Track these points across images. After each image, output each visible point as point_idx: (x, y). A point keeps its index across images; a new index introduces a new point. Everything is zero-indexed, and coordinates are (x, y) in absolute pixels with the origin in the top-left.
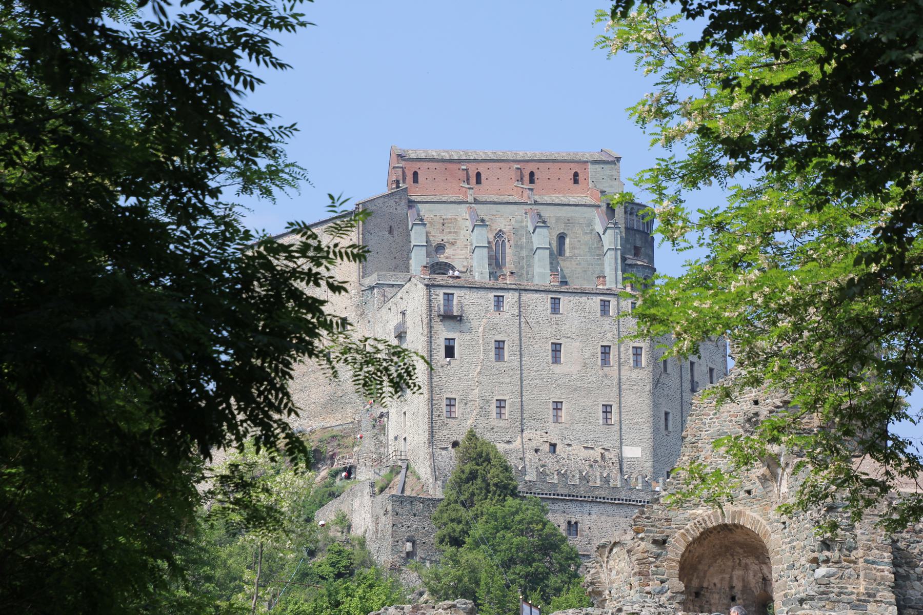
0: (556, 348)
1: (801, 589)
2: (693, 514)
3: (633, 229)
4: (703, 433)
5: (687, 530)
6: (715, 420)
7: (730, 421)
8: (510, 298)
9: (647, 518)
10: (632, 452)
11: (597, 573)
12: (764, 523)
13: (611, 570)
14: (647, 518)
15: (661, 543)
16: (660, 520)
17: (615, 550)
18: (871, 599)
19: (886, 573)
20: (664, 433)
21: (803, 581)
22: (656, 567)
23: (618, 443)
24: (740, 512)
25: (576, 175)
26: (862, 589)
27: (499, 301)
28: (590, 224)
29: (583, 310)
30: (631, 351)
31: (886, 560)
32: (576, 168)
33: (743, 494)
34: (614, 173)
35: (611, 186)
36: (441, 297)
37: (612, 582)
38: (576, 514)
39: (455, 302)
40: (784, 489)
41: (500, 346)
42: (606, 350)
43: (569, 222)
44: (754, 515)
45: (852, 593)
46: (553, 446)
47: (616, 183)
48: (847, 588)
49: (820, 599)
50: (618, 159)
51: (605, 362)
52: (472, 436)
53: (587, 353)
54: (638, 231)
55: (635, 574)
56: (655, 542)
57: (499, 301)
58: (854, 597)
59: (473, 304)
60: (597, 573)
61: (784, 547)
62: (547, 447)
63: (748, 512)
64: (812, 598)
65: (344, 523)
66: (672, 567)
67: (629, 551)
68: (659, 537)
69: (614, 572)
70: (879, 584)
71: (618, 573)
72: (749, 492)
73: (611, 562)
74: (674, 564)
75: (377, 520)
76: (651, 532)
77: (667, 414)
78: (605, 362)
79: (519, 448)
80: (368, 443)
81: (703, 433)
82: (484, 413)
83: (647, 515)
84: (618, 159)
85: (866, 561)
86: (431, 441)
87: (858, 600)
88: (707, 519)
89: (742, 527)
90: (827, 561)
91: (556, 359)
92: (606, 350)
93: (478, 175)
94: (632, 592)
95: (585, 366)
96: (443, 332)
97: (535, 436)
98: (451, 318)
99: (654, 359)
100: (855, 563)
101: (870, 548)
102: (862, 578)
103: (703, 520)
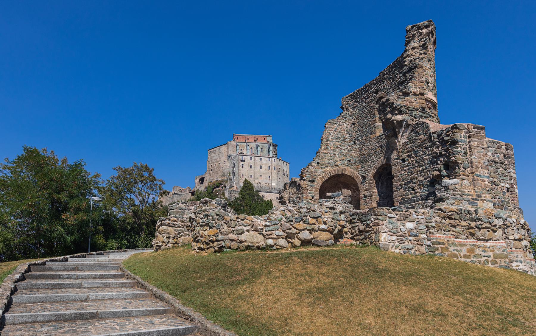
18: (479, 199)
31: (486, 175)
45: (469, 195)
48: (465, 192)
49: (452, 199)
58: (470, 197)
70: (483, 189)
87: (473, 199)
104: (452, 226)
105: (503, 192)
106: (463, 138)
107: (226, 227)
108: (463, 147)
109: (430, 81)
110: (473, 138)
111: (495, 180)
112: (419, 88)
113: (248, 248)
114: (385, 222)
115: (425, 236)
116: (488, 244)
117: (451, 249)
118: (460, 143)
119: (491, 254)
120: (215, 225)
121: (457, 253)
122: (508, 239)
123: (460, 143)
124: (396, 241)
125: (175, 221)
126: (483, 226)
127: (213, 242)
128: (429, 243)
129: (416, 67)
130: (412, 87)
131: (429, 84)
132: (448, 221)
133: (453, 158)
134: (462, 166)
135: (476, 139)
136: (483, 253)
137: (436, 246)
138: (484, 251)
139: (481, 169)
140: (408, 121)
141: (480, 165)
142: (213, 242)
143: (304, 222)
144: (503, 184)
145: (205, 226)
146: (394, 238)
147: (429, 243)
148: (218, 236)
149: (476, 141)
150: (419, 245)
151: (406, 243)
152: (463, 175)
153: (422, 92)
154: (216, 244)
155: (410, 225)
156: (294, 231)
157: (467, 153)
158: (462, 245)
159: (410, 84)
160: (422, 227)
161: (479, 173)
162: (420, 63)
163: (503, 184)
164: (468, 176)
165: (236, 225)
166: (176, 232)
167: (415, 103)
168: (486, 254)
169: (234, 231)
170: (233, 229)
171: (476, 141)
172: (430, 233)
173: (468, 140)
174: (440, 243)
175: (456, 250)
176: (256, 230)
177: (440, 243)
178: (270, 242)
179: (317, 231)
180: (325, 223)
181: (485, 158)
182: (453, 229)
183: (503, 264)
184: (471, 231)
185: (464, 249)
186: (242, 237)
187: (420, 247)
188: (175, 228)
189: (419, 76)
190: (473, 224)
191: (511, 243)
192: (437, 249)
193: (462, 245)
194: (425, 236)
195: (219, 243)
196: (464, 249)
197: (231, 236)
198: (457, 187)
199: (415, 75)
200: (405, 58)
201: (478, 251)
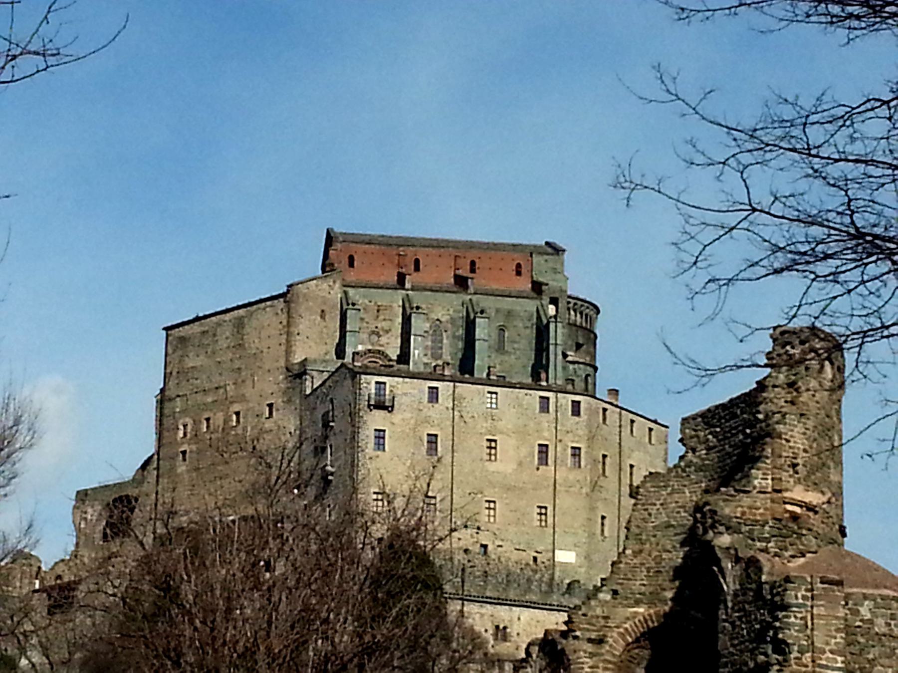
2: (636, 613)
3: (575, 325)
5: (626, 629)
6: (661, 510)
7: (678, 512)
9: (584, 615)
14: (584, 615)
15: (600, 641)
16: (598, 617)
20: (600, 538)
22: (590, 667)
23: (550, 547)
25: (519, 266)
29: (520, 405)
30: (569, 451)
31: (839, 665)
32: (519, 258)
34: (558, 266)
35: (553, 280)
36: (373, 386)
39: (387, 392)
41: (433, 439)
42: (543, 449)
43: (509, 314)
46: (485, 547)
47: (559, 276)
50: (564, 251)
53: (524, 451)
54: (581, 327)
56: (590, 640)
59: (406, 394)
62: (477, 548)
68: (593, 636)
74: (610, 666)
76: (588, 630)
77: (603, 518)
83: (584, 610)
84: (564, 251)
88: (648, 618)
92: (543, 449)
93: (417, 262)
95: (520, 464)
103: (644, 618)
106: (801, 601)
108: (799, 615)
109: (799, 461)
110: (818, 600)
112: (773, 479)
118: (794, 609)
123: (794, 609)
129: (769, 435)
130: (760, 479)
131: (799, 468)
133: (780, 636)
134: (796, 648)
135: (822, 603)
139: (831, 656)
140: (739, 551)
141: (827, 648)
149: (822, 605)
152: (796, 664)
153: (778, 488)
157: (807, 627)
159: (753, 471)
161: (824, 662)
162: (777, 426)
164: (807, 666)
167: (761, 511)
171: (822, 605)
173: (809, 603)
181: (838, 635)
189: (773, 453)
199: (765, 453)
200: (761, 403)
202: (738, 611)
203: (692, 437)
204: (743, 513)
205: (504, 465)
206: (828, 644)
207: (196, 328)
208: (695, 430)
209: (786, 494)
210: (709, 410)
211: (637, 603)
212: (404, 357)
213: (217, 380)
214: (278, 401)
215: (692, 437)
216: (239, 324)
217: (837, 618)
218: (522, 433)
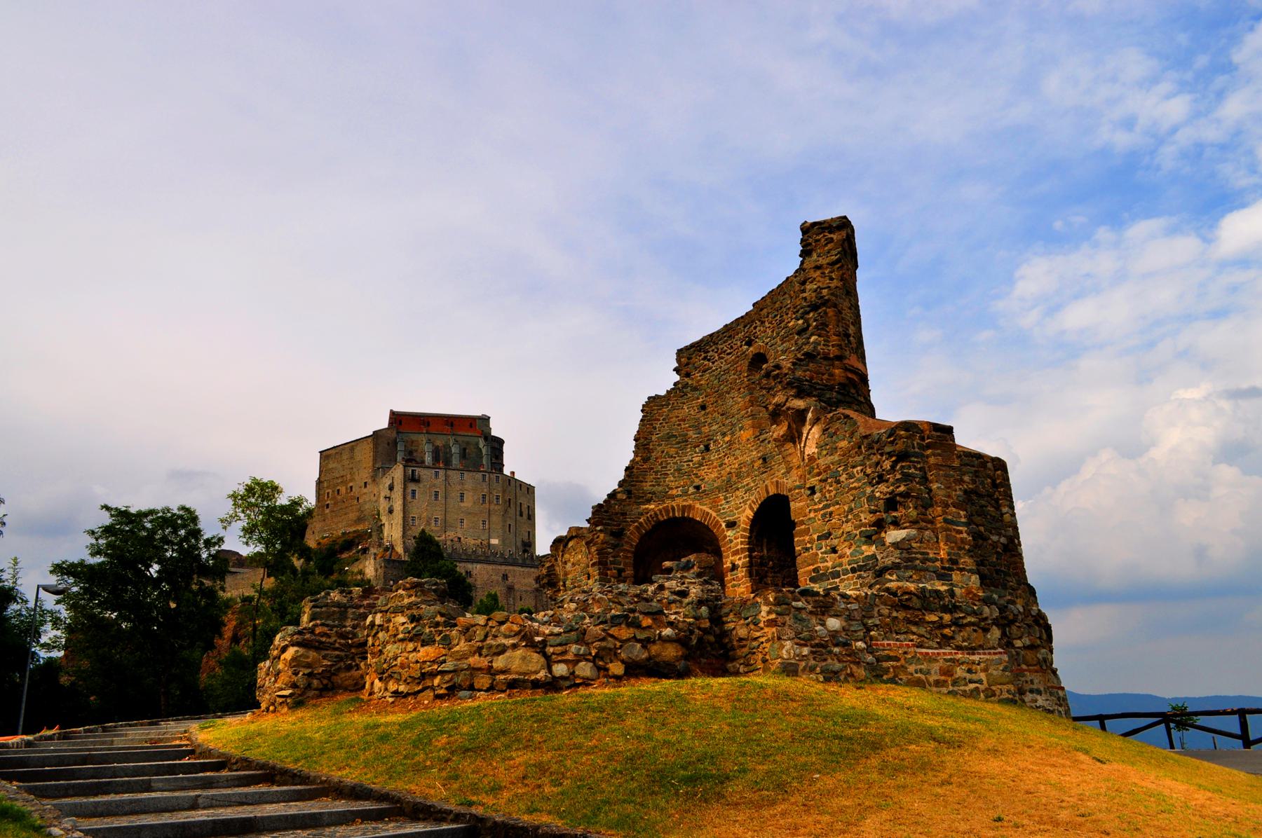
0: (462, 495)
1: (845, 560)
4: (654, 438)
8: (442, 473)
10: (494, 541)
11: (553, 566)
12: (714, 514)
13: (566, 563)
17: (571, 544)
19: (965, 535)
21: (849, 552)
24: (690, 506)
26: (943, 554)
27: (437, 474)
28: (477, 444)
33: (691, 490)
37: (566, 574)
38: (470, 566)
40: (811, 449)
43: (468, 443)
44: (704, 508)
49: (907, 568)
51: (484, 501)
52: (423, 531)
55: (593, 565)
56: (613, 534)
57: (437, 474)
58: (938, 564)
60: (553, 566)
61: (812, 515)
63: (698, 506)
64: (896, 567)
65: (361, 572)
66: (627, 557)
67: (587, 543)
69: (569, 565)
70: (960, 549)
71: (573, 564)
72: (697, 488)
73: (567, 556)
75: (376, 570)
78: (484, 501)
79: (444, 538)
80: (375, 538)
81: (654, 438)
82: (428, 523)
85: (946, 521)
86: (404, 536)
87: (943, 568)
89: (693, 520)
90: (896, 524)
91: (462, 500)
92: (484, 497)
94: (590, 582)
96: (412, 486)
97: (451, 534)
98: (414, 479)
99: (505, 501)
100: (932, 522)
101: (947, 506)
102: (942, 544)
104: (909, 622)
105: (997, 553)
107: (462, 643)
111: (982, 529)
113: (513, 685)
114: (787, 618)
115: (860, 644)
116: (976, 658)
117: (911, 669)
119: (983, 676)
120: (438, 639)
121: (923, 677)
122: (1013, 646)
124: (811, 657)
125: (325, 635)
126: (965, 621)
127: (433, 675)
128: (870, 658)
132: (901, 615)
136: (968, 676)
137: (885, 664)
138: (969, 671)
142: (433, 675)
143: (629, 625)
144: (995, 538)
145: (411, 640)
146: (805, 651)
147: (870, 658)
148: (444, 661)
150: (854, 662)
151: (830, 661)
154: (437, 681)
155: (834, 623)
156: (610, 643)
158: (931, 659)
160: (855, 626)
163: (995, 538)
165: (486, 636)
166: (326, 662)
167: (826, 377)
168: (974, 677)
169: (482, 648)
170: (480, 644)
172: (872, 638)
174: (889, 658)
175: (921, 671)
176: (532, 645)
177: (889, 658)
178: (560, 669)
179: (654, 642)
180: (671, 624)
182: (914, 629)
183: (1006, 695)
184: (947, 631)
185: (935, 667)
186: (499, 663)
187: (854, 668)
188: (324, 653)
190: (947, 617)
191: (1018, 654)
192: (887, 671)
193: (931, 659)
194: (860, 644)
195: (447, 678)
196: (935, 667)
197: (474, 660)
198: (914, 545)
201: (960, 672)
202: (819, 474)
203: (687, 364)
204: (812, 378)
205: (468, 503)
206: (949, 496)
207: (333, 452)
208: (689, 359)
209: (846, 361)
210: (702, 341)
211: (649, 501)
212: (423, 462)
213: (342, 473)
214: (369, 481)
215: (687, 364)
216: (352, 449)
217: (954, 468)
218: (475, 490)
